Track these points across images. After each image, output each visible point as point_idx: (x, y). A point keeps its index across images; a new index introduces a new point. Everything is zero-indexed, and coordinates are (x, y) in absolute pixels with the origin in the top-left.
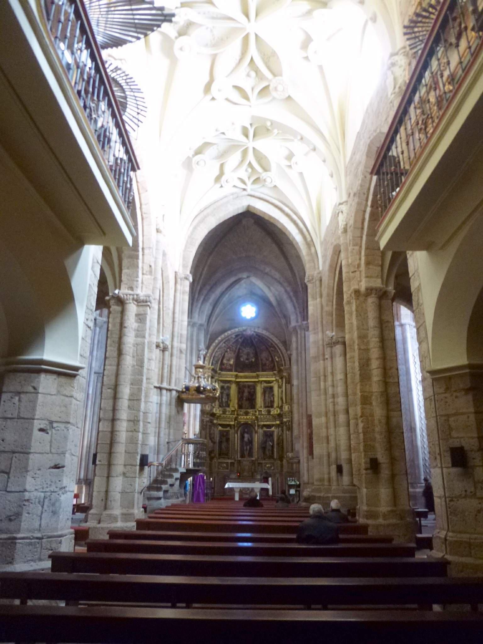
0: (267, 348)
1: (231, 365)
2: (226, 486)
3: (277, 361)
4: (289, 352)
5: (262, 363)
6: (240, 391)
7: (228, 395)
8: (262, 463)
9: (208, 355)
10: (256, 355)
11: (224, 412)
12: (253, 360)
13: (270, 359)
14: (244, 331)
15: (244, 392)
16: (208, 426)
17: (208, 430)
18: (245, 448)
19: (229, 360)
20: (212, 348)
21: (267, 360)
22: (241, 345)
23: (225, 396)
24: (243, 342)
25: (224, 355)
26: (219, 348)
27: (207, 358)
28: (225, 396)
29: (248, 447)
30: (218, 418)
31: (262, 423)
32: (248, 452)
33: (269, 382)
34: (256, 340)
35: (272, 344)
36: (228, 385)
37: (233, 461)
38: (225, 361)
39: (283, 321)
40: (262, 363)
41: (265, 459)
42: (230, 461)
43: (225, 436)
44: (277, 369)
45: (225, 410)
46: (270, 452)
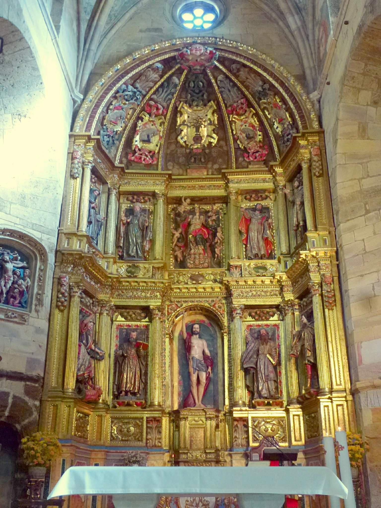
0: (250, 105)
1: (152, 153)
2: (62, 488)
3: (276, 136)
4: (314, 96)
5: (237, 149)
6: (179, 221)
7: (144, 229)
8: (245, 420)
9: (85, 106)
10: (221, 128)
11: (131, 274)
12: (214, 141)
13: (259, 138)
14: (187, 46)
15: (189, 224)
16: (76, 300)
17: (75, 312)
18: (194, 378)
19: (148, 141)
20: (96, 89)
21: (249, 138)
22: (179, 99)
23: (135, 232)
24: (184, 88)
25: (135, 126)
26: (115, 97)
27: (82, 113)
28: (135, 232)
29: (203, 376)
30: (115, 285)
31: (244, 302)
32: (202, 389)
33: (257, 194)
34: (220, 77)
35: (265, 81)
36: (148, 206)
37: (156, 414)
38: (137, 141)
39: (293, 21)
40: (237, 149)
41: (252, 406)
42: (146, 415)
43: (134, 348)
44: (277, 156)
45: (135, 267)
46: (272, 385)
